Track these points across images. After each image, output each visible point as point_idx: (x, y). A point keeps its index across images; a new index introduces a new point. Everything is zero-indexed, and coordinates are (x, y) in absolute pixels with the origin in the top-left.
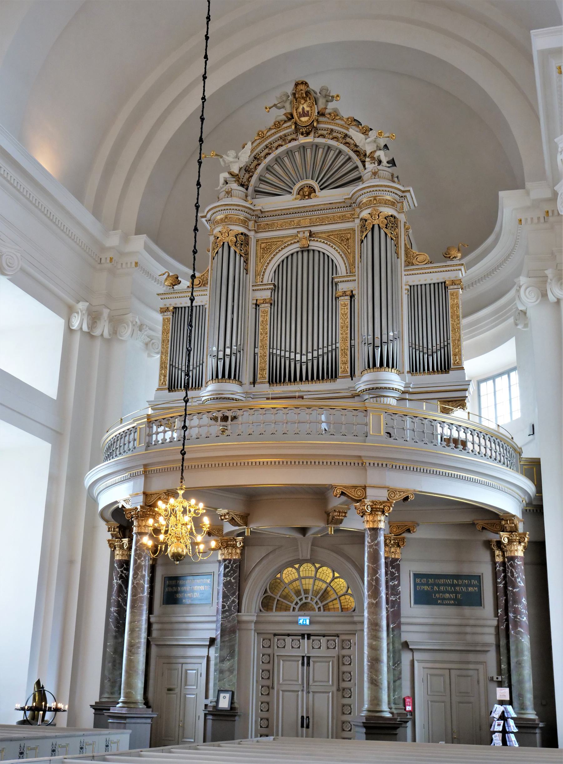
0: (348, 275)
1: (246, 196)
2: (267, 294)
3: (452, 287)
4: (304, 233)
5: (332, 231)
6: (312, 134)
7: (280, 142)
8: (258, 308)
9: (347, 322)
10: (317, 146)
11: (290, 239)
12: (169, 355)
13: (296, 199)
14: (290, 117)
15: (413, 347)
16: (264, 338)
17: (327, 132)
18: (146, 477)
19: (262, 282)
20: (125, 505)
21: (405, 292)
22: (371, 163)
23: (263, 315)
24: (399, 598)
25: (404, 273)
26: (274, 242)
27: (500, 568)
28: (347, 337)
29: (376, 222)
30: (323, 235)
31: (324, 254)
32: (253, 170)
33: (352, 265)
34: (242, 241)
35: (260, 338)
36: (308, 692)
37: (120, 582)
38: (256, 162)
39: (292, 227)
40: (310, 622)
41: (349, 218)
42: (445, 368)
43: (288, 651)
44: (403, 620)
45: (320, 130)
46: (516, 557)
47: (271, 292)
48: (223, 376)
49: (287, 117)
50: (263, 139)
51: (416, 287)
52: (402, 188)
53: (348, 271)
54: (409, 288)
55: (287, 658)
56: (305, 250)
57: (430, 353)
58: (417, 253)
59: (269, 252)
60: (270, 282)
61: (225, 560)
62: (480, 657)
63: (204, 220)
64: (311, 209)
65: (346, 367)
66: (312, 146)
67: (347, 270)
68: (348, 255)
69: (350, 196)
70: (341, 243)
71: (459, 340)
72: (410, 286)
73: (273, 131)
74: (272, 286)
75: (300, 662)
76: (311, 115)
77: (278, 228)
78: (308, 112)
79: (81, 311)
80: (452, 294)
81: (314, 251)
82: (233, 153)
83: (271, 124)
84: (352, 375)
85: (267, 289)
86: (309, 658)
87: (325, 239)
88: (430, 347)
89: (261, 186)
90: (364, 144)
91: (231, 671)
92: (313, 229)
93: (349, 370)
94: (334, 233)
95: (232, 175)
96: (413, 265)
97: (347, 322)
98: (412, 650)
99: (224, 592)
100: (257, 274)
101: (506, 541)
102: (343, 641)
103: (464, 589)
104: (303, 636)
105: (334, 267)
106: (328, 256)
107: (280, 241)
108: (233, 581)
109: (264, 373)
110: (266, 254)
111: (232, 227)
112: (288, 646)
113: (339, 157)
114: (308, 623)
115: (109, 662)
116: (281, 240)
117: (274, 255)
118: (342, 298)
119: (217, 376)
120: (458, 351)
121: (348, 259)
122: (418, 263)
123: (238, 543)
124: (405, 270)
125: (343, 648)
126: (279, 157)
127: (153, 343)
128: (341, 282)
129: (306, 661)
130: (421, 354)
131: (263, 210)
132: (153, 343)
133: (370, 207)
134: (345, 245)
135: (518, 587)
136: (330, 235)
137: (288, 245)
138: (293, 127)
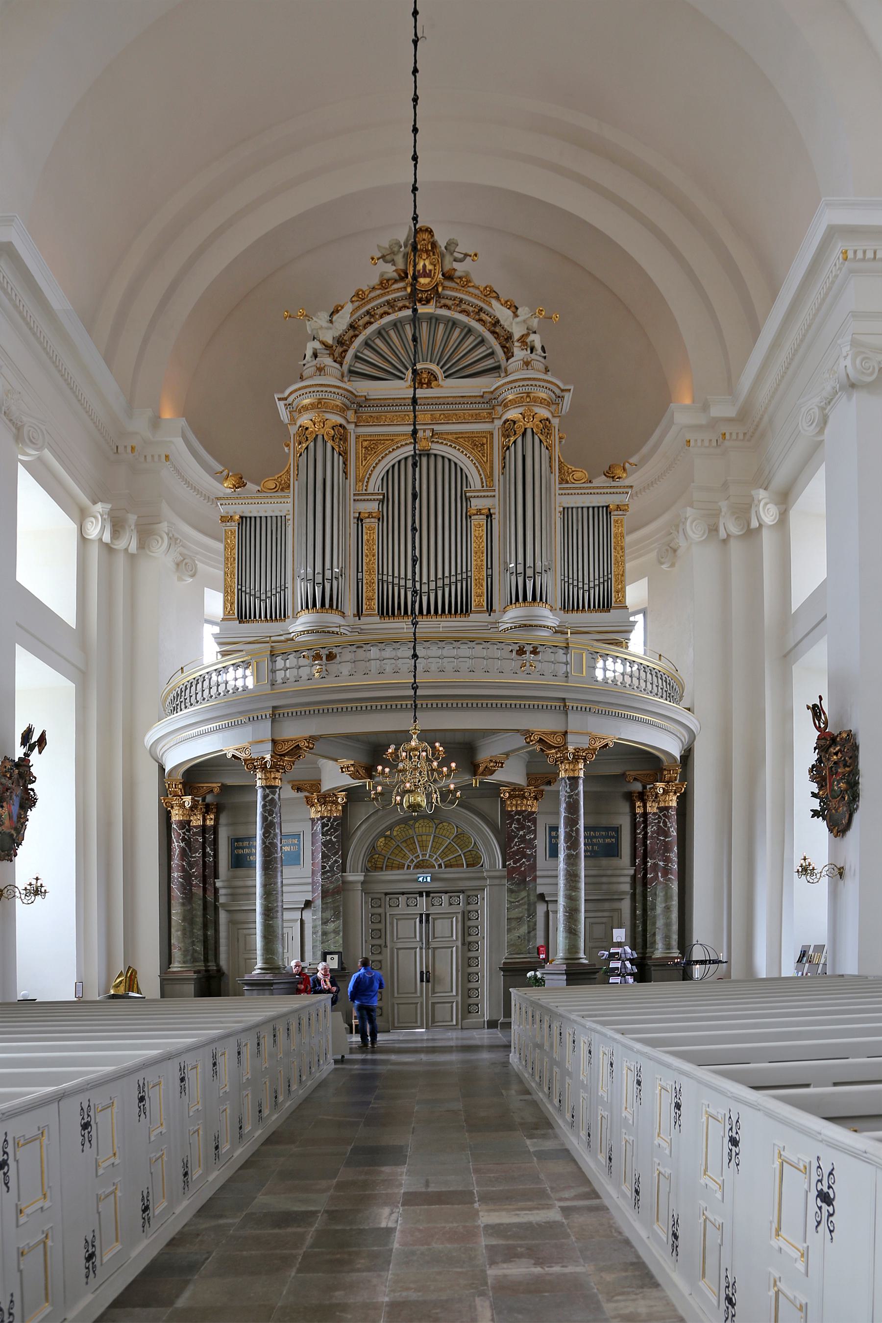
0: (485, 488)
1: (343, 376)
2: (373, 507)
3: (616, 513)
4: (424, 431)
5: (462, 433)
6: (433, 303)
7: (386, 309)
9: (483, 547)
10: (437, 319)
11: (403, 438)
12: (236, 577)
15: (566, 581)
16: (370, 560)
17: (454, 302)
19: (366, 490)
21: (558, 515)
23: (369, 532)
25: (558, 492)
26: (380, 440)
28: (482, 565)
29: (528, 426)
30: (450, 437)
31: (450, 460)
32: (348, 342)
34: (341, 435)
35: (364, 561)
38: (351, 333)
39: (406, 423)
41: (484, 418)
42: (605, 605)
45: (443, 298)
47: (379, 505)
48: (323, 604)
49: (399, 275)
50: (363, 301)
51: (570, 510)
53: (484, 484)
54: (562, 509)
58: (573, 469)
59: (375, 452)
60: (376, 491)
63: (282, 403)
64: (434, 401)
65: (482, 600)
66: (431, 319)
67: (482, 483)
69: (492, 389)
70: (473, 449)
71: (622, 575)
72: (564, 508)
73: (378, 292)
76: (434, 276)
77: (386, 423)
78: (430, 271)
79: (102, 516)
81: (436, 455)
82: (326, 316)
83: (375, 281)
84: (490, 609)
85: (374, 500)
87: (451, 441)
88: (586, 581)
89: (357, 365)
92: (436, 428)
93: (485, 604)
94: (464, 436)
95: (325, 346)
96: (567, 482)
97: (483, 547)
100: (358, 480)
105: (464, 477)
106: (456, 464)
107: (390, 440)
109: (373, 603)
110: (369, 455)
113: (467, 337)
116: (391, 438)
117: (383, 458)
118: (476, 517)
119: (314, 605)
120: (622, 588)
121: (484, 470)
122: (573, 481)
126: (384, 329)
128: (475, 497)
130: (576, 589)
131: (367, 397)
133: (522, 406)
134: (479, 451)
136: (459, 438)
137: (402, 445)
138: (409, 290)
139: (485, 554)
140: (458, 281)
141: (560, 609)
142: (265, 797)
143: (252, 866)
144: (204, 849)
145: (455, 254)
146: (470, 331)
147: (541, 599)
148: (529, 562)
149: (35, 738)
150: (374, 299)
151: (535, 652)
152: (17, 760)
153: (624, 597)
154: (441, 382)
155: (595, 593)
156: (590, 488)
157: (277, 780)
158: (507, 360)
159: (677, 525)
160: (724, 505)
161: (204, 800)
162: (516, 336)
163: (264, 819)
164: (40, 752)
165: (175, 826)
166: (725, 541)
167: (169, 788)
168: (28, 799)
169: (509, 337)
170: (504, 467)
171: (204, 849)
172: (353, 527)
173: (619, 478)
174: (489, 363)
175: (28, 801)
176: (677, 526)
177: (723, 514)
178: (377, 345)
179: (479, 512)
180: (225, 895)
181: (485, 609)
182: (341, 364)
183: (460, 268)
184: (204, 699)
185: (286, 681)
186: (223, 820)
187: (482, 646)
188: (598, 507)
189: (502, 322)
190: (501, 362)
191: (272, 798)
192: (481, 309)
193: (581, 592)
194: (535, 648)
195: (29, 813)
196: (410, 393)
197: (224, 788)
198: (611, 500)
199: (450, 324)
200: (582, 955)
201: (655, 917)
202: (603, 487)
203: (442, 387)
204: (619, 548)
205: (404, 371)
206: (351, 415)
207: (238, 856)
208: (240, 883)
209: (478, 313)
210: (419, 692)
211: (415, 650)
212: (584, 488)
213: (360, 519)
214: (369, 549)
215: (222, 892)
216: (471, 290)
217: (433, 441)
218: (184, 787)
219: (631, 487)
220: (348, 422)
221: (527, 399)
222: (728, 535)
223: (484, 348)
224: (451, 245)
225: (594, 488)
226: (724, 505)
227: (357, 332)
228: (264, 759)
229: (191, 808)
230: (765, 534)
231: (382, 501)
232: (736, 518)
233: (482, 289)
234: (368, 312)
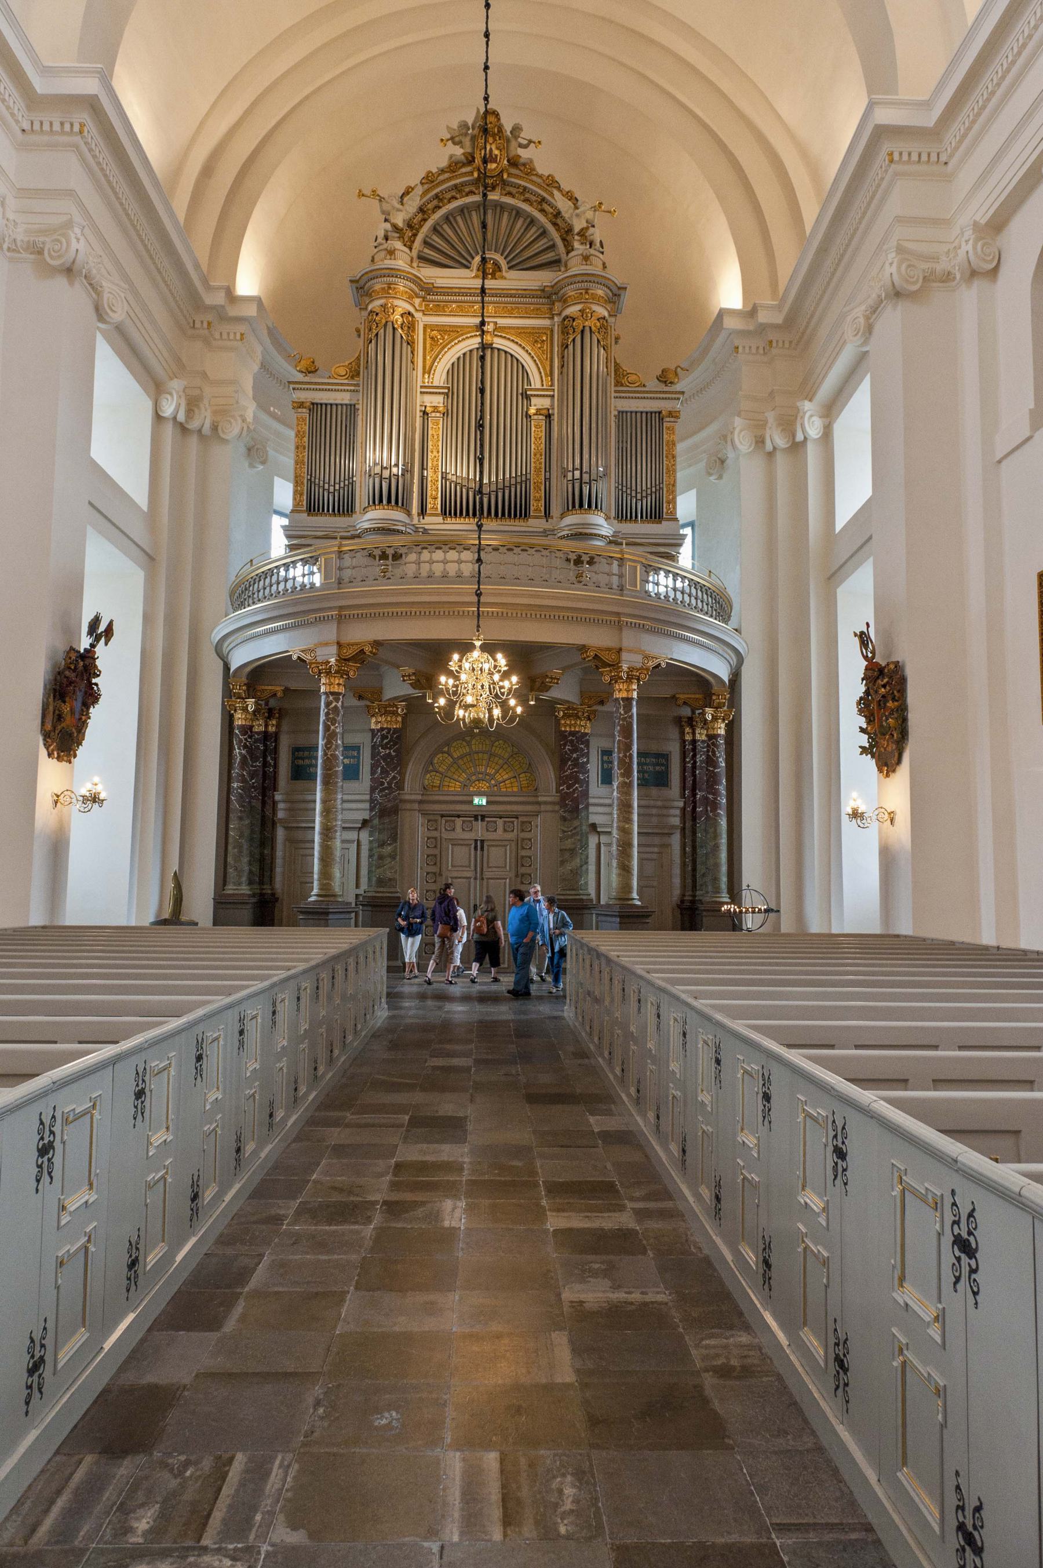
0: (545, 387)
1: (412, 261)
2: (438, 400)
3: (668, 419)
5: (523, 328)
6: (498, 189)
8: (426, 417)
10: (502, 207)
14: (470, 160)
18: (339, 623)
19: (432, 383)
20: (303, 656)
21: (613, 418)
22: (582, 244)
24: (588, 777)
25: (613, 395)
27: (689, 747)
28: (540, 468)
35: (429, 457)
40: (487, 802)
43: (459, 834)
44: (591, 801)
46: (719, 735)
49: (467, 158)
53: (544, 383)
57: (639, 496)
60: (442, 385)
61: (382, 729)
66: (496, 206)
71: (674, 485)
72: (619, 412)
73: (447, 175)
74: (446, 391)
75: (473, 846)
79: (177, 393)
80: (668, 428)
81: (499, 350)
83: (444, 163)
84: (547, 515)
90: (572, 216)
93: (542, 509)
96: (622, 385)
98: (599, 833)
99: (382, 768)
101: (709, 717)
102: (523, 822)
103: (651, 768)
104: (476, 817)
108: (393, 754)
112: (458, 829)
115: (234, 848)
123: (399, 710)
124: (616, 392)
125: (523, 831)
127: (257, 449)
130: (629, 498)
132: (257, 449)
135: (719, 767)
138: (476, 175)
139: (543, 457)
140: (522, 168)
141: (614, 518)
142: (328, 704)
143: (313, 778)
144: (265, 757)
145: (520, 140)
146: (532, 221)
147: (596, 507)
149: (102, 628)
151: (591, 562)
152: (82, 651)
153: (675, 508)
154: (504, 274)
155: (647, 503)
156: (644, 392)
157: (341, 687)
158: (568, 253)
159: (725, 437)
160: (771, 417)
161: (267, 704)
162: (577, 230)
163: (327, 728)
164: (106, 644)
165: (237, 732)
166: (771, 455)
167: (233, 689)
168: (91, 695)
169: (570, 230)
170: (563, 366)
171: (265, 757)
173: (671, 383)
174: (550, 256)
175: (92, 697)
176: (725, 437)
177: (769, 425)
178: (444, 230)
180: (285, 810)
181: (543, 514)
182: (411, 249)
183: (524, 154)
184: (265, 598)
185: (352, 580)
186: (285, 727)
187: (540, 553)
188: (651, 413)
189: (563, 214)
190: (562, 255)
191: (336, 706)
192: (543, 199)
193: (634, 501)
194: (592, 558)
195: (91, 710)
196: (477, 283)
197: (287, 690)
198: (664, 406)
199: (514, 213)
202: (656, 392)
203: (505, 278)
204: (670, 457)
205: (469, 259)
207: (298, 766)
208: (300, 797)
209: (540, 203)
210: (482, 599)
211: (479, 555)
212: (638, 392)
215: (281, 806)
216: (534, 178)
217: (496, 335)
218: (248, 690)
219: (683, 393)
222: (775, 448)
223: (545, 240)
224: (516, 129)
225: (647, 392)
226: (771, 417)
227: (426, 216)
228: (329, 662)
229: (254, 712)
230: (811, 448)
231: (447, 394)
232: (782, 430)
233: (545, 178)
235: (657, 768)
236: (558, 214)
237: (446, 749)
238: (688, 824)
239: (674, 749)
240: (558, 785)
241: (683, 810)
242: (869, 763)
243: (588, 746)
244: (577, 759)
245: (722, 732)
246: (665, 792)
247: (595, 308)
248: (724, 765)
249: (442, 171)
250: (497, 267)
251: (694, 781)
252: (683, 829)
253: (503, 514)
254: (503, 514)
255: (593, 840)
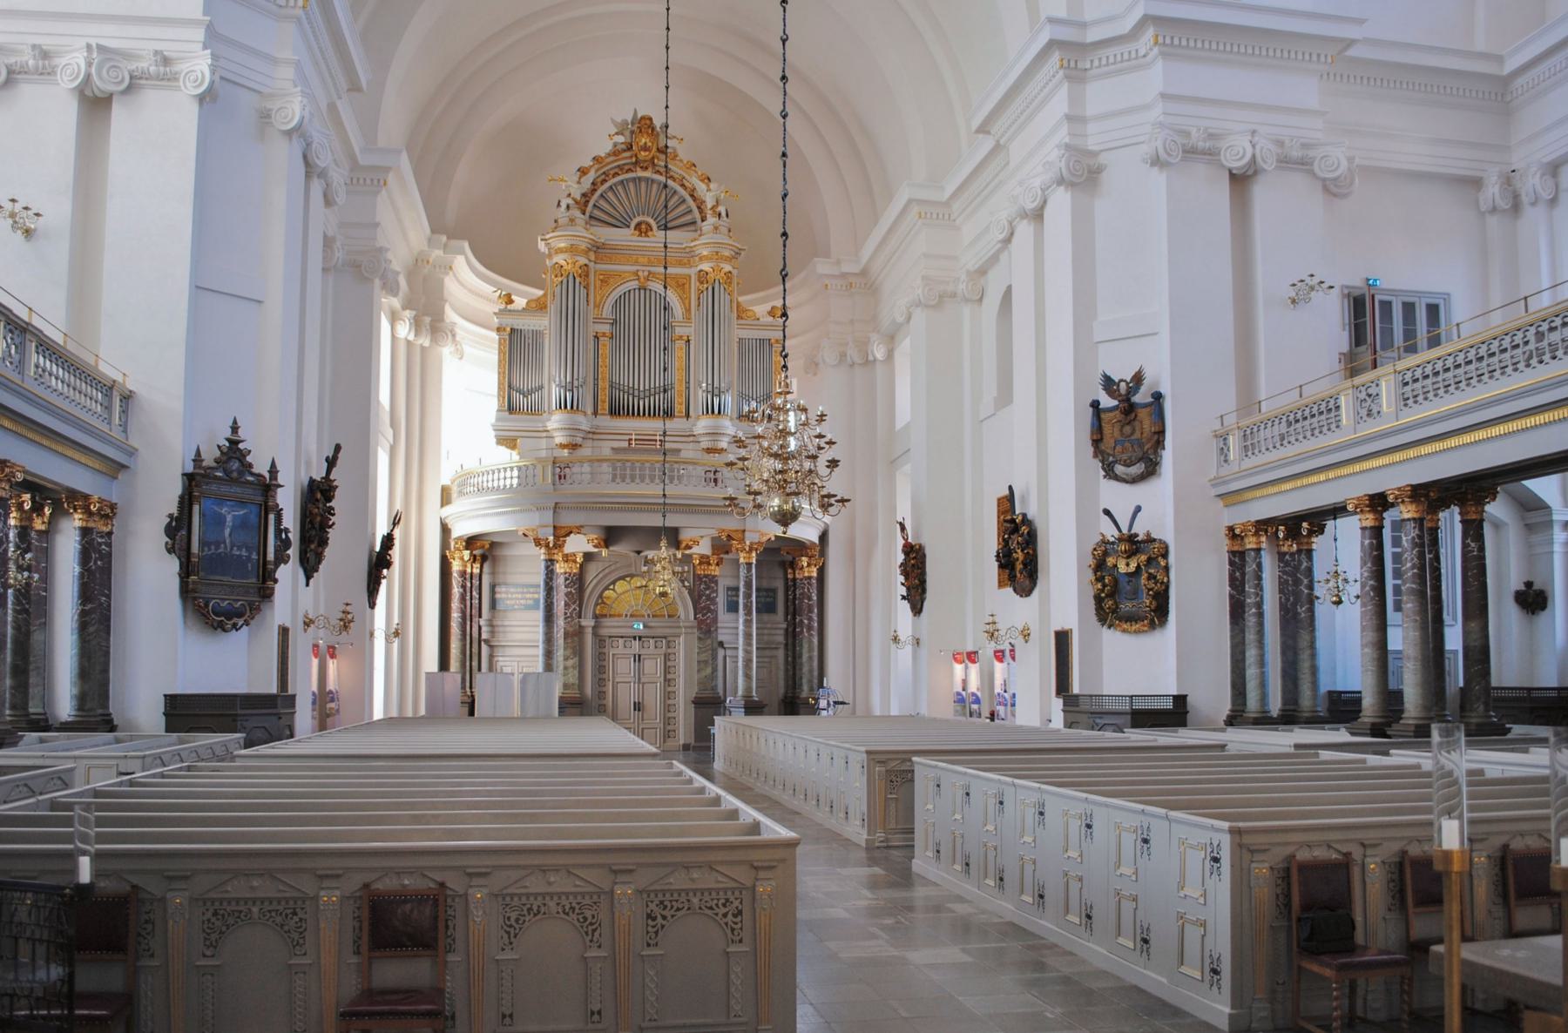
2: (606, 328)
6: (650, 169)
7: (616, 170)
13: (633, 235)
14: (630, 148)
33: (688, 310)
36: (639, 682)
37: (461, 590)
40: (644, 627)
43: (621, 650)
44: (719, 625)
52: (739, 246)
55: (625, 656)
56: (642, 288)
61: (566, 573)
62: (774, 652)
68: (685, 300)
84: (688, 416)
86: (639, 656)
91: (574, 667)
92: (652, 269)
100: (596, 306)
111: (578, 258)
114: (641, 627)
119: (566, 407)
121: (684, 304)
129: (638, 658)
138: (634, 160)
148: (716, 384)
150: (609, 163)
154: (655, 233)
158: (703, 221)
172: (591, 346)
174: (688, 218)
179: (681, 338)
200: (754, 694)
201: (801, 664)
206: (592, 256)
213: (596, 337)
214: (603, 361)
220: (590, 261)
221: (717, 257)
234: (604, 173)
235: (768, 600)
236: (694, 189)
237: (612, 587)
238: (790, 641)
239: (779, 585)
240: (695, 615)
241: (787, 630)
242: (906, 605)
243: (717, 585)
244: (709, 595)
245: (815, 574)
246: (772, 617)
247: (722, 265)
248: (815, 598)
249: (609, 155)
250: (650, 228)
251: (795, 609)
252: (786, 645)
253: (654, 414)
254: (654, 414)
255: (721, 652)
